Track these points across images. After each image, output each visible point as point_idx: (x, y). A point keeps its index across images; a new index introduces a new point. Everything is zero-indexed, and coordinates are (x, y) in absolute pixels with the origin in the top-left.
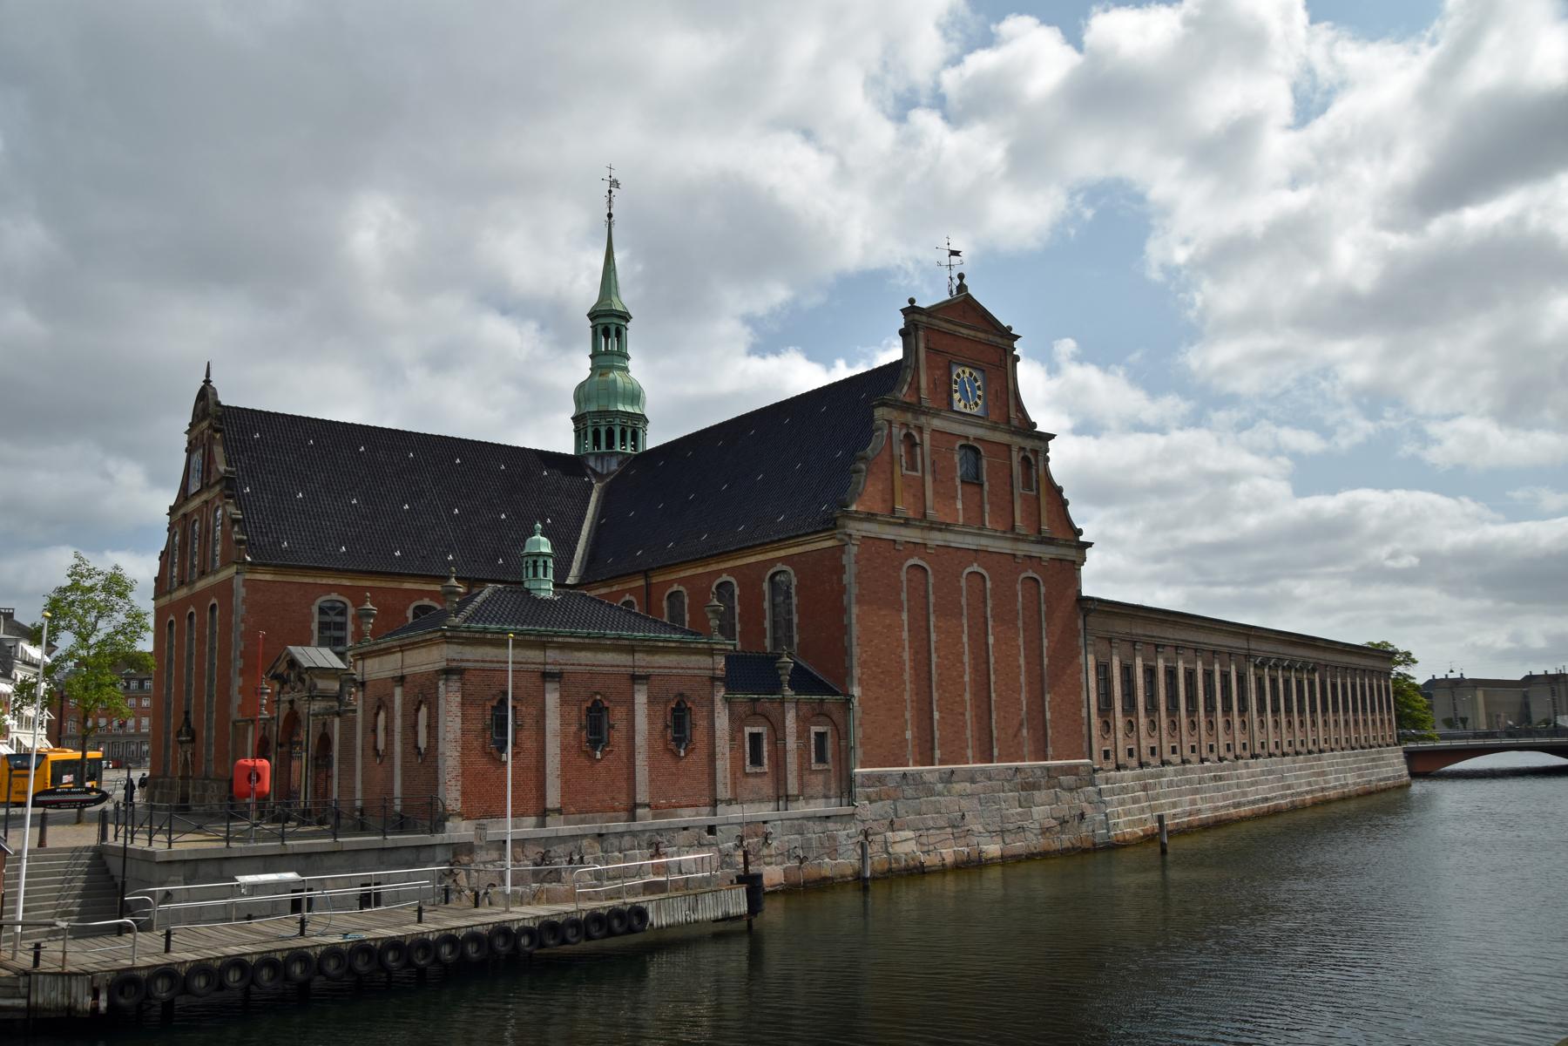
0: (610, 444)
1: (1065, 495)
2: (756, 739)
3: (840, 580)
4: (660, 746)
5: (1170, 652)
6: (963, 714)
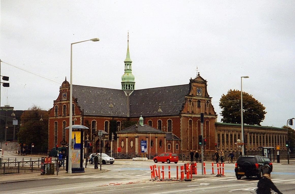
1: (214, 107)
2: (169, 145)
3: (180, 122)
4: (158, 146)
5: (231, 132)
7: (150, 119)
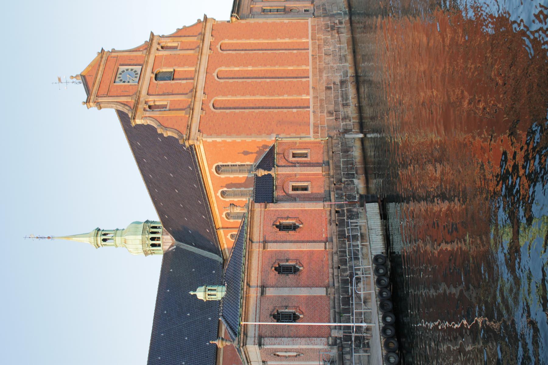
0: (158, 239)
1: (181, 27)
2: (295, 189)
6: (286, 82)
7: (221, 217)
